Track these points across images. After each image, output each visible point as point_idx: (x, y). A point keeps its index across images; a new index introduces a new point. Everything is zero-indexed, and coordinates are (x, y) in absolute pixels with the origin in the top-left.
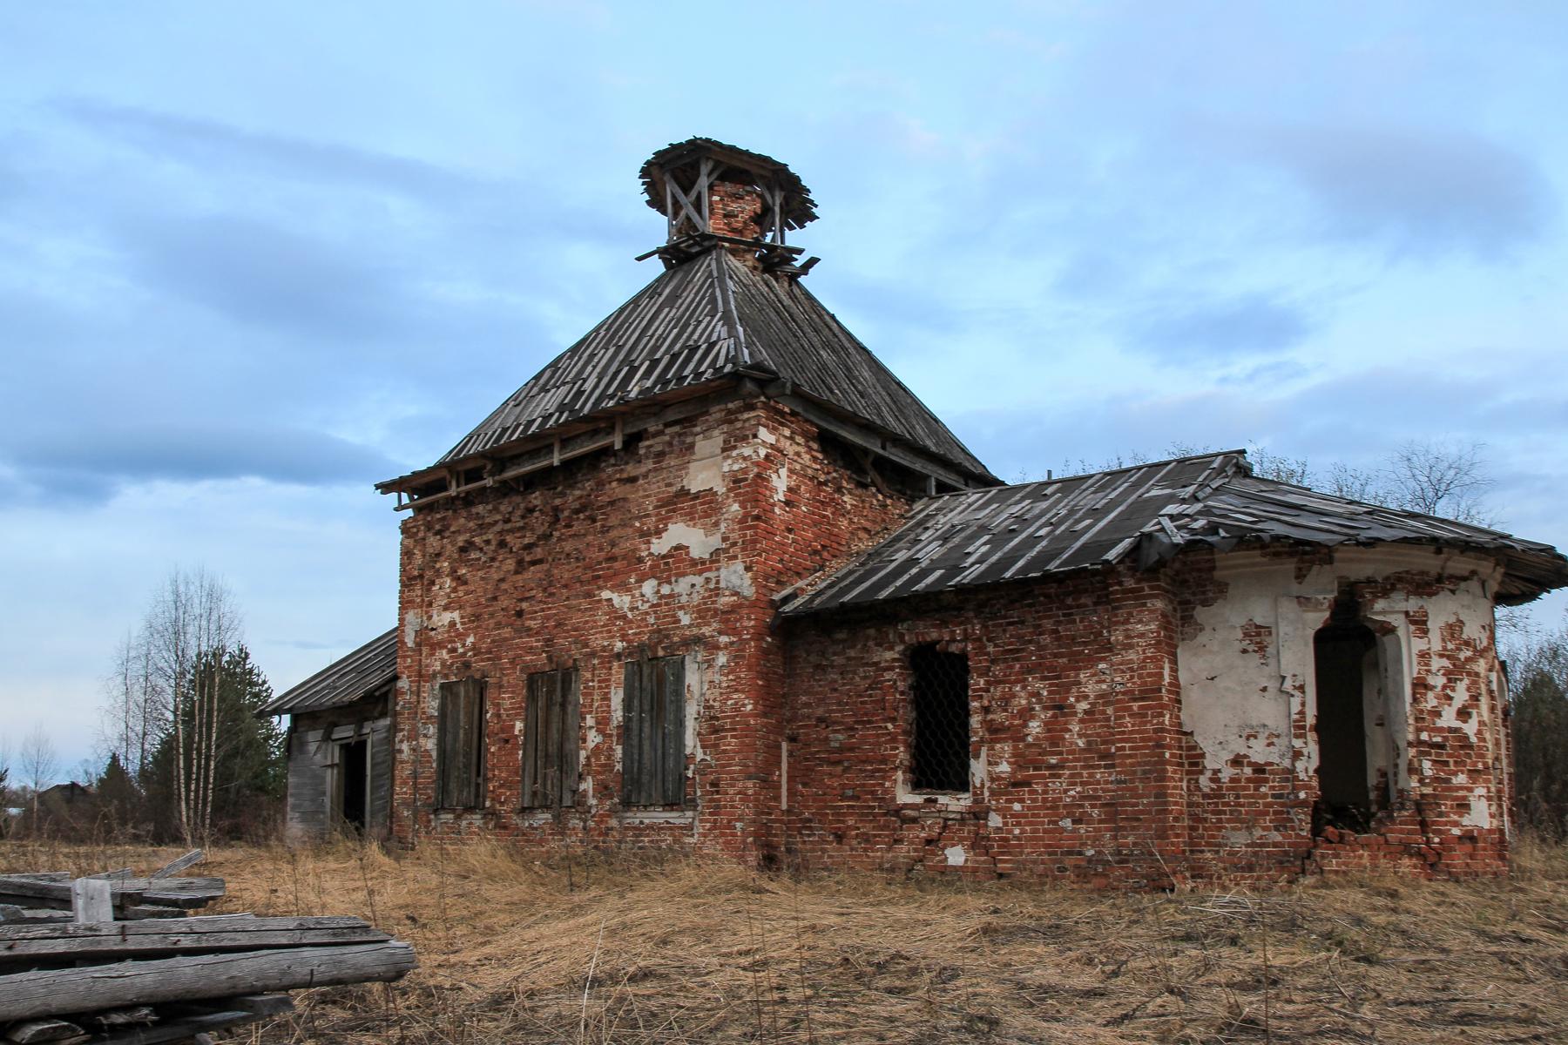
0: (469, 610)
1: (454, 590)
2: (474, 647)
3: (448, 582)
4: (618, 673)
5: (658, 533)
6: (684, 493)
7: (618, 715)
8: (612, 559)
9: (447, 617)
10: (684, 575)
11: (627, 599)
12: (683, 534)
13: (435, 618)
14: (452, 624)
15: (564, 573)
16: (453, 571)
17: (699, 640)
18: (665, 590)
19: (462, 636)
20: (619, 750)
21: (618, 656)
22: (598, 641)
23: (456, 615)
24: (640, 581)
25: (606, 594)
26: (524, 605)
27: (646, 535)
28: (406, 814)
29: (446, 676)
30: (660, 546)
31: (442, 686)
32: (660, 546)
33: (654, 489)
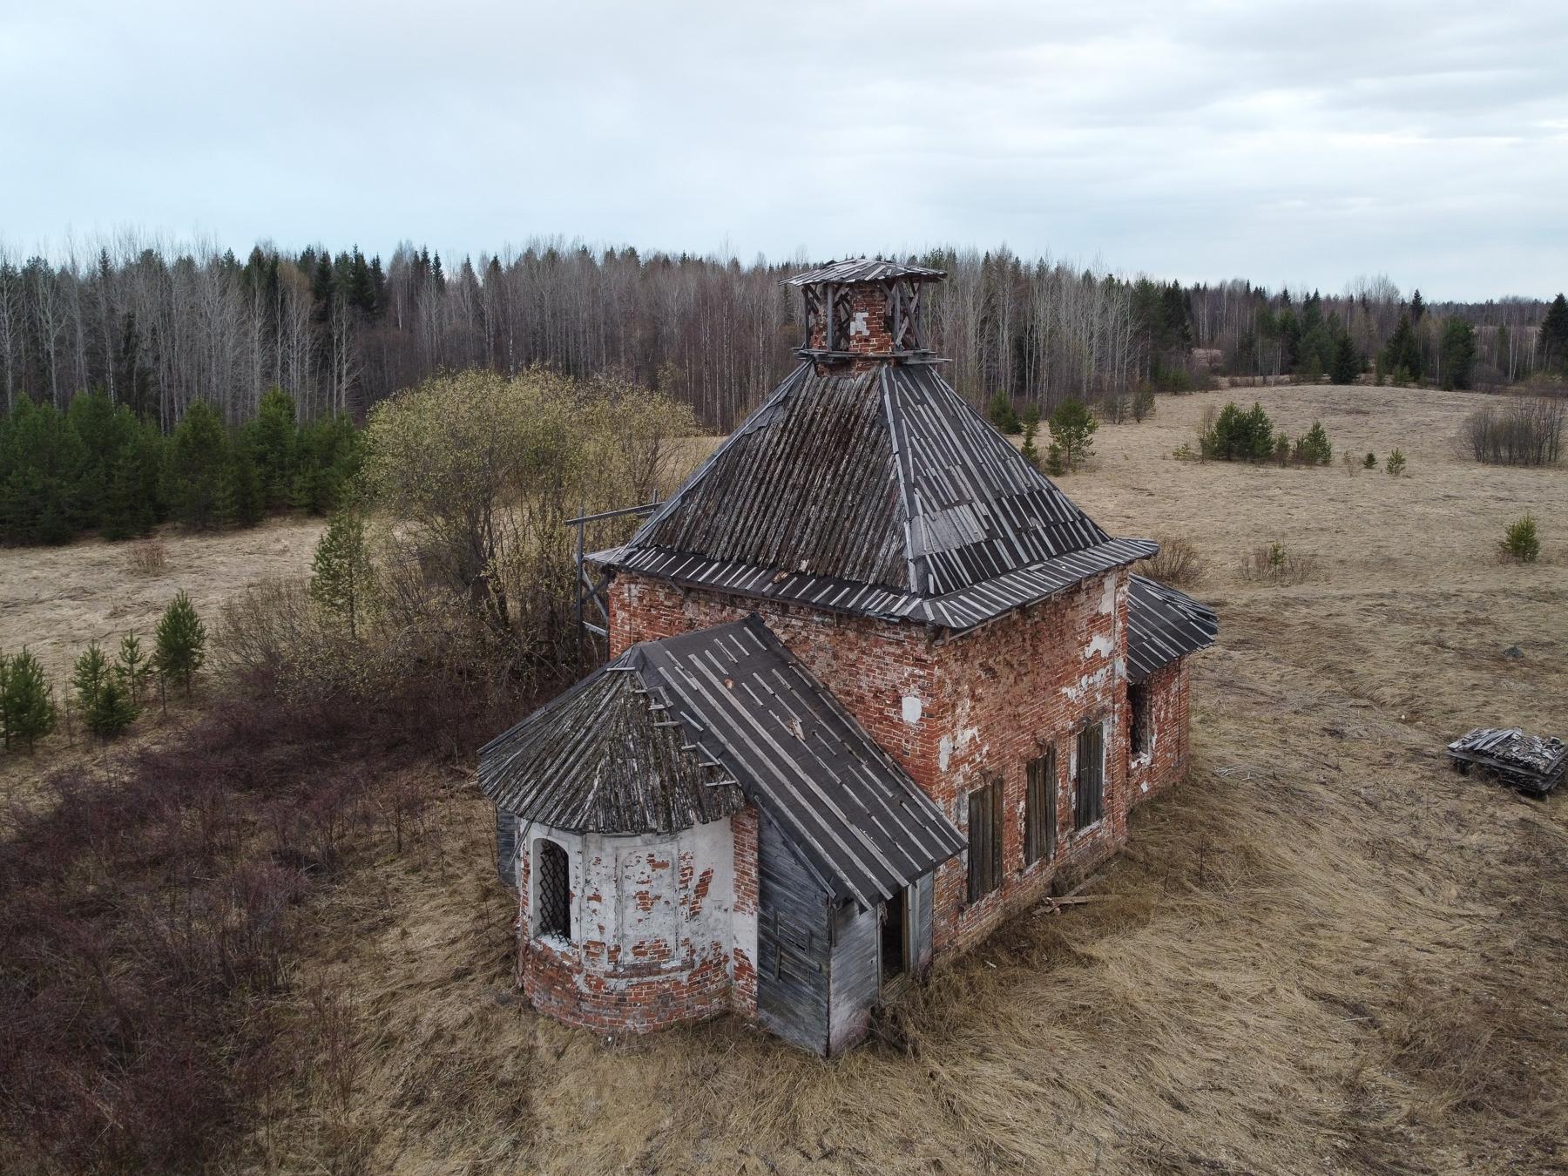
0: (983, 723)
1: (973, 708)
2: (989, 755)
3: (968, 703)
4: (1073, 743)
5: (1088, 642)
6: (1097, 614)
7: (1073, 772)
8: (1066, 663)
9: (969, 733)
10: (1097, 669)
11: (1074, 691)
12: (1101, 644)
13: (959, 737)
14: (973, 738)
15: (1042, 680)
16: (972, 691)
17: (1104, 711)
18: (1091, 681)
19: (979, 747)
20: (1074, 795)
21: (1072, 732)
22: (1059, 725)
23: (975, 730)
24: (1081, 676)
25: (1064, 690)
26: (1020, 710)
27: (1082, 644)
28: (942, 923)
29: (972, 786)
30: (1089, 652)
31: (972, 797)
32: (1089, 652)
33: (1086, 612)
